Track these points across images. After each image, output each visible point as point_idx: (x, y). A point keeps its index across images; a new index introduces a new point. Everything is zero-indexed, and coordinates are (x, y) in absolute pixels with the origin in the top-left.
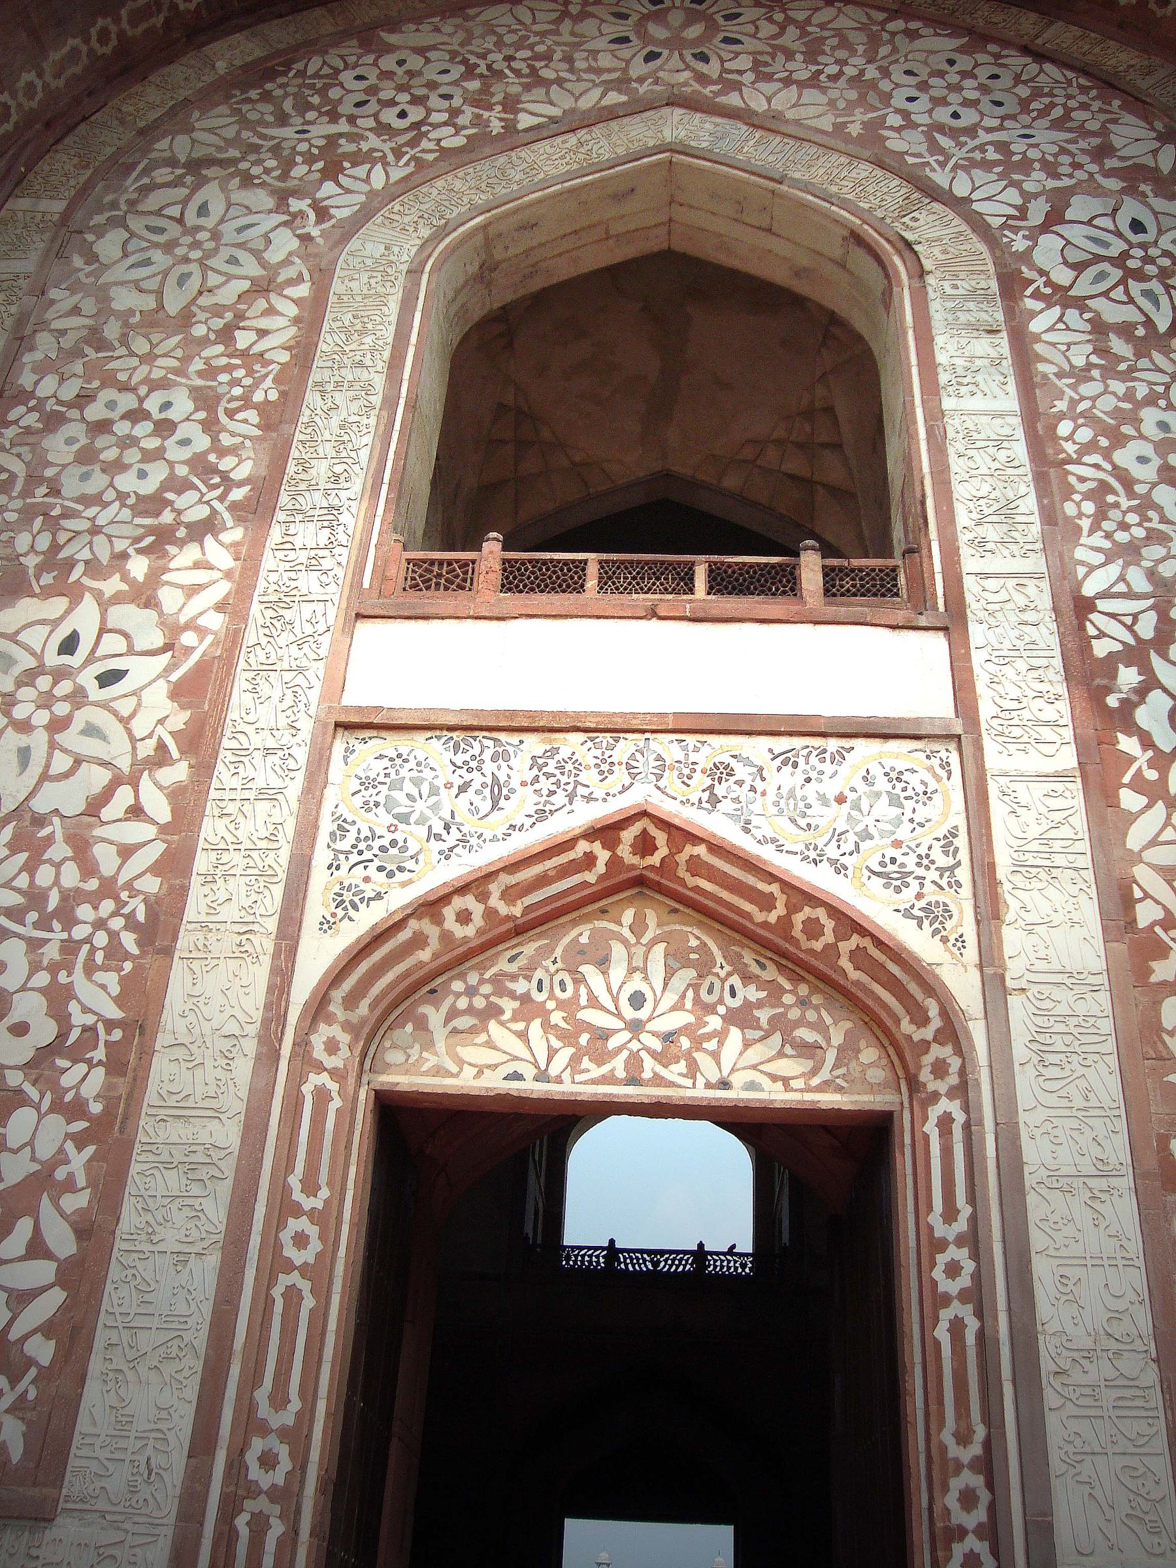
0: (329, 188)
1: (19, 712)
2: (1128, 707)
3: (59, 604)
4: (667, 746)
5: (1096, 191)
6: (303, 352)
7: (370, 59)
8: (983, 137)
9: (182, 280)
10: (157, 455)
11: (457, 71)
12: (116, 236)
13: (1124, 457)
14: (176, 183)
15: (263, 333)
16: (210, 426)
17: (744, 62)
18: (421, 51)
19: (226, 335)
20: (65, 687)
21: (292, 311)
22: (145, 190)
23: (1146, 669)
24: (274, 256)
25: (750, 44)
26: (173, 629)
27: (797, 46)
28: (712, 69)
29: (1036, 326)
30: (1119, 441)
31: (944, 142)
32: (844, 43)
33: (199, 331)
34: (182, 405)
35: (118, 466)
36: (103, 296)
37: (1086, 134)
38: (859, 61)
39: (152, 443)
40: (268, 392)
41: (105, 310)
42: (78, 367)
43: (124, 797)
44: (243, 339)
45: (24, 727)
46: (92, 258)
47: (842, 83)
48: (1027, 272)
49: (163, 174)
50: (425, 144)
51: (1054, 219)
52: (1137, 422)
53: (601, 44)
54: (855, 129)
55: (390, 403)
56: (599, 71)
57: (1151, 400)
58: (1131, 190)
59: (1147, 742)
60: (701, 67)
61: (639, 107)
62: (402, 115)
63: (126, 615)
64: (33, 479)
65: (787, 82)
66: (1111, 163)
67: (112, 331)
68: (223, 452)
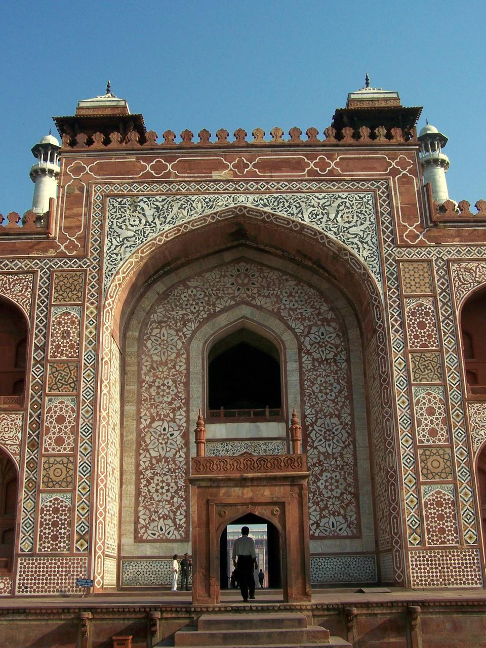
0: (185, 329)
1: (160, 441)
2: (310, 433)
3: (160, 423)
4: (248, 443)
5: (316, 325)
6: (188, 369)
7: (186, 291)
8: (298, 311)
9: (164, 352)
10: (168, 393)
11: (203, 294)
12: (149, 342)
13: (314, 388)
14: (157, 328)
15: (180, 366)
16: (176, 387)
17: (255, 291)
18: (195, 288)
19: (174, 367)
20: (166, 437)
21: (184, 361)
22: (152, 329)
23: (313, 427)
24: (179, 348)
25: (257, 285)
26: (179, 426)
27: (265, 285)
28: (249, 293)
29: (303, 360)
30: (314, 384)
31: (291, 313)
32: (274, 284)
33: (170, 366)
34: (171, 383)
35: (163, 396)
36: (150, 356)
37: (316, 309)
38: (276, 289)
39: (167, 391)
40: (184, 380)
41: (153, 361)
42: (151, 374)
43: (178, 454)
44: (178, 368)
45: (161, 443)
46: (147, 348)
47: (274, 296)
48: (303, 347)
49: (154, 325)
50: (200, 317)
51: (309, 333)
52: (317, 380)
53: (228, 285)
54: (276, 310)
55: (203, 382)
56: (229, 294)
57: (320, 376)
58: (322, 324)
59: (312, 439)
60: (247, 292)
61: (237, 304)
62: (195, 308)
63: (171, 424)
64: (151, 399)
65: (264, 296)
66: (320, 317)
67: (155, 366)
68: (179, 393)
